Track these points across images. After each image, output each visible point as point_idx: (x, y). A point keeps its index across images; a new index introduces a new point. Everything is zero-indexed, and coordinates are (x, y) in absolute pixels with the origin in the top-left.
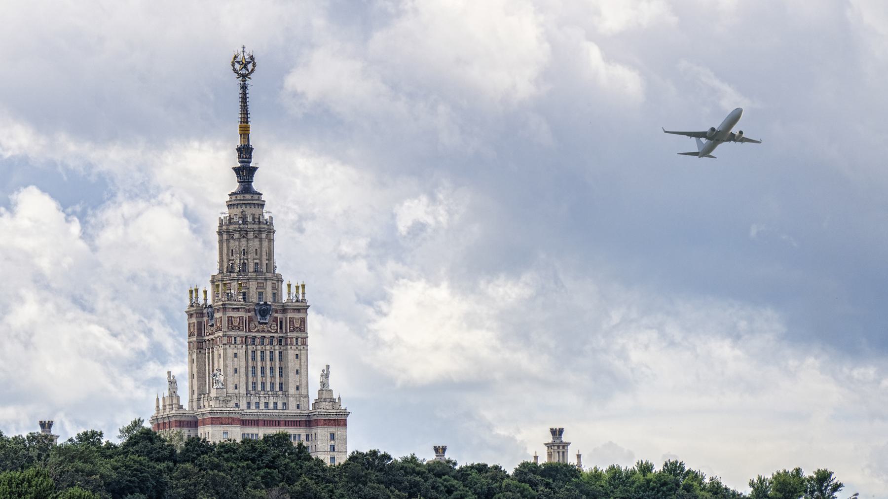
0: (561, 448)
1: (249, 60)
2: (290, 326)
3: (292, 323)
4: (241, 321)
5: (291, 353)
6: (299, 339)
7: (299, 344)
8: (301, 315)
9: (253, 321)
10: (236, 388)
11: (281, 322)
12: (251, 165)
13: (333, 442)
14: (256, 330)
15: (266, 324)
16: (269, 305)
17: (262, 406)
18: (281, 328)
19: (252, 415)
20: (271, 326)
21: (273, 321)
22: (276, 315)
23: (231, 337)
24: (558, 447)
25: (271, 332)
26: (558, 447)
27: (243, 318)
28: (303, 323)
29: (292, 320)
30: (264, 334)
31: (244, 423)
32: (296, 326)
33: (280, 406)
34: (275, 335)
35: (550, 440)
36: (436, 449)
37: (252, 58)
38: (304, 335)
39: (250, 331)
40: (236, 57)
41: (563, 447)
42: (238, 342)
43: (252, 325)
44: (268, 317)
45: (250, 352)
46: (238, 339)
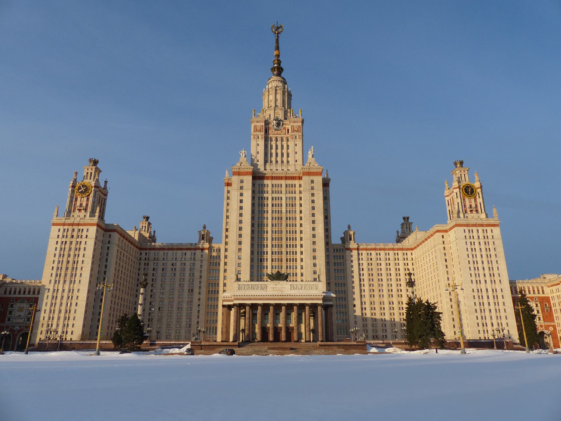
0: (462, 171)
2: (291, 129)
4: (262, 128)
11: (288, 130)
13: (312, 185)
14: (273, 134)
16: (279, 120)
22: (285, 126)
25: (281, 134)
27: (263, 126)
32: (295, 129)
34: (285, 136)
36: (404, 218)
37: (281, 27)
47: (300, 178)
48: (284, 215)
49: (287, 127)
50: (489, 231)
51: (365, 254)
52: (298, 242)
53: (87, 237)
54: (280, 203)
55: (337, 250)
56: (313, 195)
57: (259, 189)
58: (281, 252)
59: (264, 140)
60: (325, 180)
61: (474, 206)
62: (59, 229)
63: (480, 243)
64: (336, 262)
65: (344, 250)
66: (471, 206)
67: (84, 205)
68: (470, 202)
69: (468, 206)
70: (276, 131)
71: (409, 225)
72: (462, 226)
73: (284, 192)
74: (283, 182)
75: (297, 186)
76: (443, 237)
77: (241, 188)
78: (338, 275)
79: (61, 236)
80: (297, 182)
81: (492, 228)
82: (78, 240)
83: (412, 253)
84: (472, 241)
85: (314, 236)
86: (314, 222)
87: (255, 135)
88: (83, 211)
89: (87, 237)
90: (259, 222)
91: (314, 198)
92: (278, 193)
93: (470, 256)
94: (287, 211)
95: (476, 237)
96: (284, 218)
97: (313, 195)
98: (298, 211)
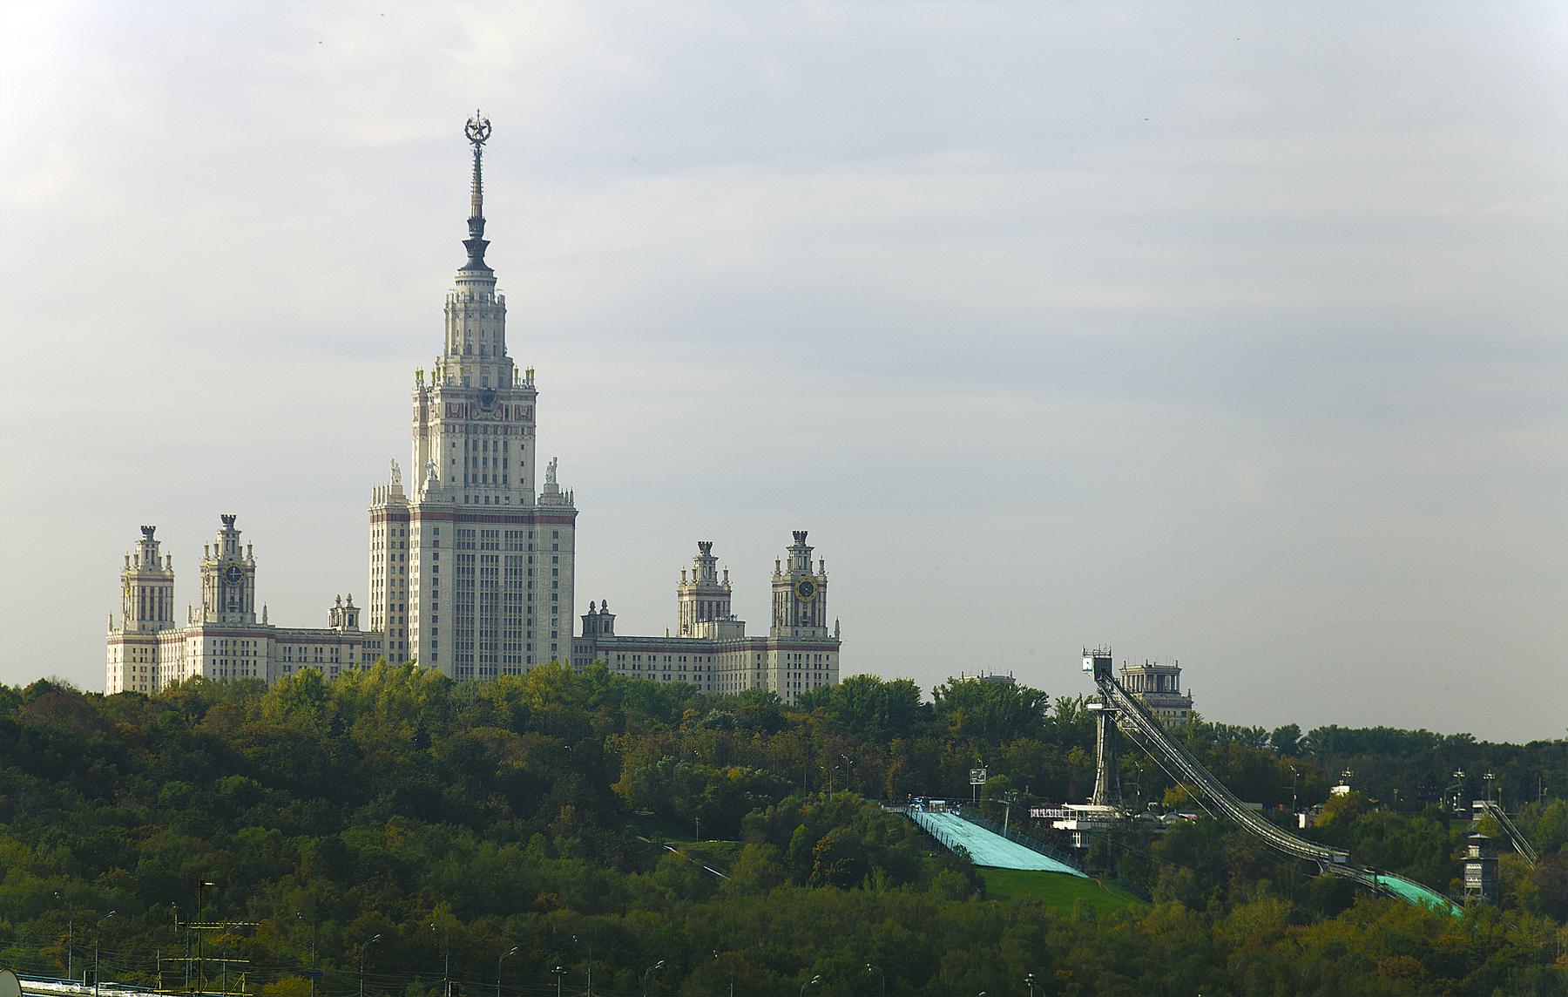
1: (485, 125)
5: (514, 444)
6: (526, 429)
8: (531, 403)
10: (453, 481)
11: (507, 410)
12: (483, 238)
15: (489, 411)
17: (482, 500)
18: (507, 416)
23: (449, 425)
25: (494, 420)
29: (518, 407)
30: (487, 423)
33: (502, 499)
34: (501, 423)
35: (792, 542)
37: (487, 122)
38: (531, 424)
39: (471, 419)
40: (469, 121)
41: (806, 552)
42: (457, 431)
45: (471, 441)
46: (457, 427)
47: (530, 519)
49: (505, 403)
50: (824, 658)
52: (524, 641)
53: (255, 655)
54: (494, 567)
55: (581, 647)
56: (555, 560)
58: (496, 657)
61: (809, 614)
62: (215, 641)
63: (808, 674)
65: (594, 648)
66: (805, 613)
67: (237, 599)
69: (801, 614)
71: (710, 563)
74: (502, 528)
75: (525, 535)
76: (759, 658)
77: (436, 544)
79: (218, 652)
80: (524, 528)
81: (828, 653)
82: (243, 658)
83: (709, 658)
84: (797, 671)
85: (554, 634)
86: (555, 609)
87: (449, 425)
88: (237, 611)
89: (255, 655)
91: (558, 566)
95: (804, 666)
96: (502, 596)
97: (555, 560)
98: (525, 584)
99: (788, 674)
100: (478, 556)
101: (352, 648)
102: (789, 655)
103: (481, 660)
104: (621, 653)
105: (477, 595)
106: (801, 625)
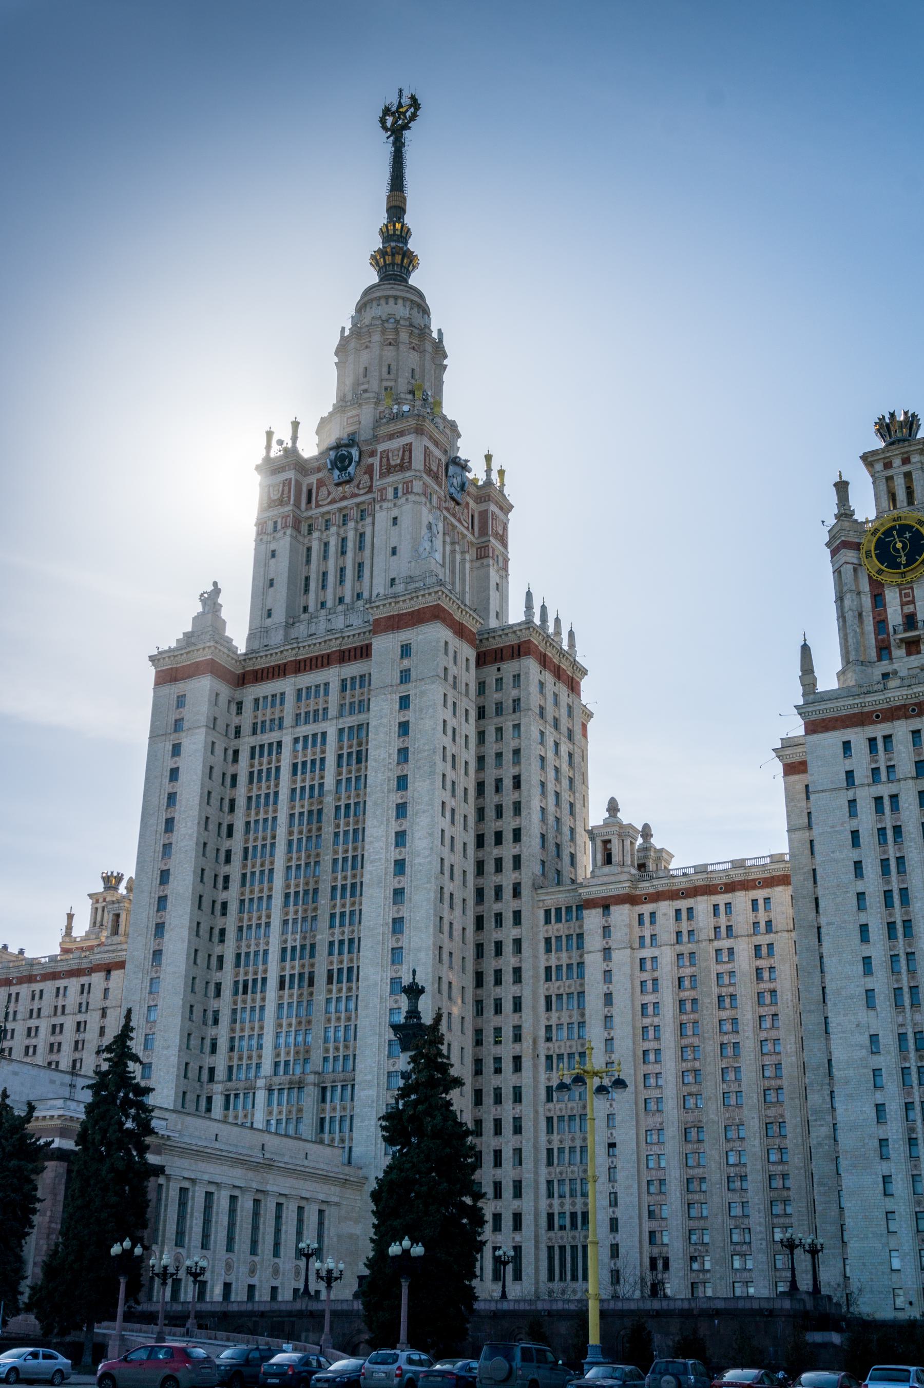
0: (897, 462)
2: (381, 466)
3: (384, 460)
6: (400, 486)
7: (400, 494)
9: (325, 485)
13: (406, 663)
14: (329, 500)
15: (348, 482)
19: (271, 655)
20: (360, 483)
21: (365, 473)
24: (888, 465)
25: (357, 495)
26: (888, 465)
28: (407, 453)
29: (385, 455)
30: (344, 503)
31: (259, 675)
32: (393, 463)
39: (318, 506)
43: (324, 491)
44: (351, 469)
48: (329, 801)
51: (665, 914)
56: (405, 702)
57: (256, 717)
58: (313, 946)
59: (289, 531)
60: (515, 632)
64: (553, 963)
68: (908, 603)
70: (340, 488)
72: (834, 728)
73: (333, 711)
74: (332, 675)
78: (559, 1018)
84: (885, 790)
85: (400, 866)
90: (247, 841)
92: (315, 720)
93: (872, 869)
94: (339, 782)
97: (405, 702)
99: (852, 803)
100: (287, 741)
101: (107, 978)
102: (847, 745)
103: (283, 959)
104: (646, 909)
105: (282, 819)
106: (899, 652)
